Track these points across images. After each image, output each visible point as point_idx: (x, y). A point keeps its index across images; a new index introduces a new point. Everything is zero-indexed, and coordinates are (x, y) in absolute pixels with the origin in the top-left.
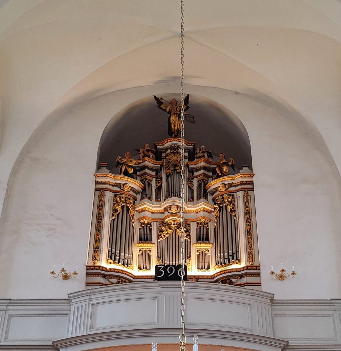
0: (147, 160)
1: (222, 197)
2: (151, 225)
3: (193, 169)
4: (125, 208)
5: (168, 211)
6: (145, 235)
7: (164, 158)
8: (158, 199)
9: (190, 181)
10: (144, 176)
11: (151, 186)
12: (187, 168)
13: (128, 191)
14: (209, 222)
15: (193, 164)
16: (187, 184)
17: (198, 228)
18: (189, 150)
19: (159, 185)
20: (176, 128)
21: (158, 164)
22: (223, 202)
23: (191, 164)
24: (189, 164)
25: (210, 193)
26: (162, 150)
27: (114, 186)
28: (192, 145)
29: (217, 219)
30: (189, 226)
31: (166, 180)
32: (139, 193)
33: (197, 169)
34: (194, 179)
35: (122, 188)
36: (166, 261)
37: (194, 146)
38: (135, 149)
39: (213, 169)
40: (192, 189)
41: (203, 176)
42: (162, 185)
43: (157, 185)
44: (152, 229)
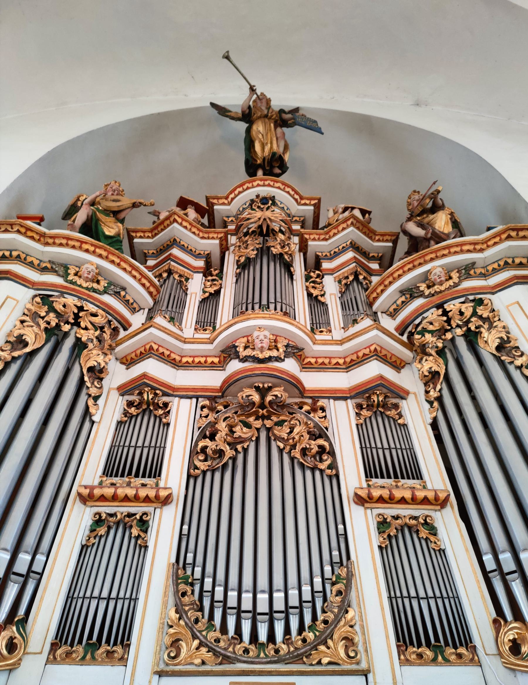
0: (179, 220)
1: (440, 312)
2: (169, 412)
3: (320, 254)
4: (69, 343)
5: (237, 356)
6: (132, 450)
7: (232, 235)
8: (205, 328)
9: (314, 282)
10: (164, 266)
11: (186, 294)
12: (302, 254)
13: (95, 291)
14: (404, 401)
15: (321, 239)
16: (305, 288)
17: (361, 421)
18: (302, 219)
19: (212, 290)
20: (267, 149)
21: (213, 238)
22: (449, 325)
23: (312, 237)
24: (307, 236)
25: (385, 313)
26: (228, 217)
27: (44, 270)
28: (313, 202)
29: (438, 387)
30: (324, 414)
31: (235, 279)
32: (142, 311)
33: (331, 255)
34: (325, 276)
35: (70, 278)
36: (219, 590)
37: (317, 207)
38: (149, 213)
39: (380, 255)
40: (320, 301)
41: (354, 264)
42: (222, 290)
43: (206, 290)
44: (168, 424)
